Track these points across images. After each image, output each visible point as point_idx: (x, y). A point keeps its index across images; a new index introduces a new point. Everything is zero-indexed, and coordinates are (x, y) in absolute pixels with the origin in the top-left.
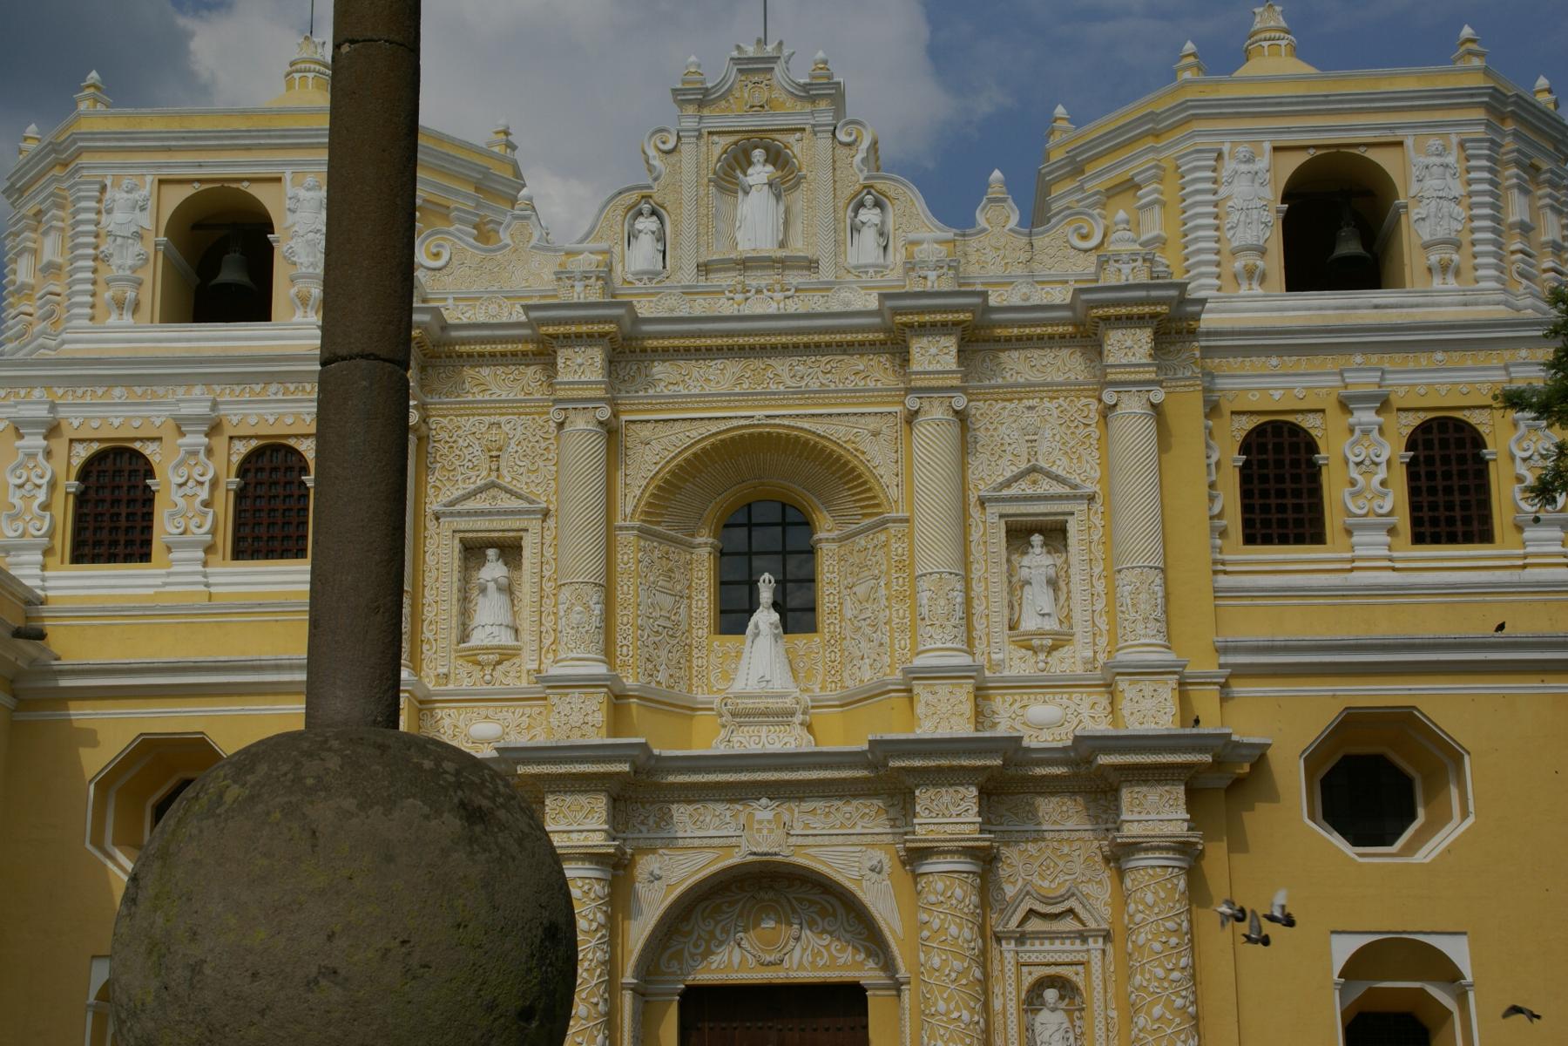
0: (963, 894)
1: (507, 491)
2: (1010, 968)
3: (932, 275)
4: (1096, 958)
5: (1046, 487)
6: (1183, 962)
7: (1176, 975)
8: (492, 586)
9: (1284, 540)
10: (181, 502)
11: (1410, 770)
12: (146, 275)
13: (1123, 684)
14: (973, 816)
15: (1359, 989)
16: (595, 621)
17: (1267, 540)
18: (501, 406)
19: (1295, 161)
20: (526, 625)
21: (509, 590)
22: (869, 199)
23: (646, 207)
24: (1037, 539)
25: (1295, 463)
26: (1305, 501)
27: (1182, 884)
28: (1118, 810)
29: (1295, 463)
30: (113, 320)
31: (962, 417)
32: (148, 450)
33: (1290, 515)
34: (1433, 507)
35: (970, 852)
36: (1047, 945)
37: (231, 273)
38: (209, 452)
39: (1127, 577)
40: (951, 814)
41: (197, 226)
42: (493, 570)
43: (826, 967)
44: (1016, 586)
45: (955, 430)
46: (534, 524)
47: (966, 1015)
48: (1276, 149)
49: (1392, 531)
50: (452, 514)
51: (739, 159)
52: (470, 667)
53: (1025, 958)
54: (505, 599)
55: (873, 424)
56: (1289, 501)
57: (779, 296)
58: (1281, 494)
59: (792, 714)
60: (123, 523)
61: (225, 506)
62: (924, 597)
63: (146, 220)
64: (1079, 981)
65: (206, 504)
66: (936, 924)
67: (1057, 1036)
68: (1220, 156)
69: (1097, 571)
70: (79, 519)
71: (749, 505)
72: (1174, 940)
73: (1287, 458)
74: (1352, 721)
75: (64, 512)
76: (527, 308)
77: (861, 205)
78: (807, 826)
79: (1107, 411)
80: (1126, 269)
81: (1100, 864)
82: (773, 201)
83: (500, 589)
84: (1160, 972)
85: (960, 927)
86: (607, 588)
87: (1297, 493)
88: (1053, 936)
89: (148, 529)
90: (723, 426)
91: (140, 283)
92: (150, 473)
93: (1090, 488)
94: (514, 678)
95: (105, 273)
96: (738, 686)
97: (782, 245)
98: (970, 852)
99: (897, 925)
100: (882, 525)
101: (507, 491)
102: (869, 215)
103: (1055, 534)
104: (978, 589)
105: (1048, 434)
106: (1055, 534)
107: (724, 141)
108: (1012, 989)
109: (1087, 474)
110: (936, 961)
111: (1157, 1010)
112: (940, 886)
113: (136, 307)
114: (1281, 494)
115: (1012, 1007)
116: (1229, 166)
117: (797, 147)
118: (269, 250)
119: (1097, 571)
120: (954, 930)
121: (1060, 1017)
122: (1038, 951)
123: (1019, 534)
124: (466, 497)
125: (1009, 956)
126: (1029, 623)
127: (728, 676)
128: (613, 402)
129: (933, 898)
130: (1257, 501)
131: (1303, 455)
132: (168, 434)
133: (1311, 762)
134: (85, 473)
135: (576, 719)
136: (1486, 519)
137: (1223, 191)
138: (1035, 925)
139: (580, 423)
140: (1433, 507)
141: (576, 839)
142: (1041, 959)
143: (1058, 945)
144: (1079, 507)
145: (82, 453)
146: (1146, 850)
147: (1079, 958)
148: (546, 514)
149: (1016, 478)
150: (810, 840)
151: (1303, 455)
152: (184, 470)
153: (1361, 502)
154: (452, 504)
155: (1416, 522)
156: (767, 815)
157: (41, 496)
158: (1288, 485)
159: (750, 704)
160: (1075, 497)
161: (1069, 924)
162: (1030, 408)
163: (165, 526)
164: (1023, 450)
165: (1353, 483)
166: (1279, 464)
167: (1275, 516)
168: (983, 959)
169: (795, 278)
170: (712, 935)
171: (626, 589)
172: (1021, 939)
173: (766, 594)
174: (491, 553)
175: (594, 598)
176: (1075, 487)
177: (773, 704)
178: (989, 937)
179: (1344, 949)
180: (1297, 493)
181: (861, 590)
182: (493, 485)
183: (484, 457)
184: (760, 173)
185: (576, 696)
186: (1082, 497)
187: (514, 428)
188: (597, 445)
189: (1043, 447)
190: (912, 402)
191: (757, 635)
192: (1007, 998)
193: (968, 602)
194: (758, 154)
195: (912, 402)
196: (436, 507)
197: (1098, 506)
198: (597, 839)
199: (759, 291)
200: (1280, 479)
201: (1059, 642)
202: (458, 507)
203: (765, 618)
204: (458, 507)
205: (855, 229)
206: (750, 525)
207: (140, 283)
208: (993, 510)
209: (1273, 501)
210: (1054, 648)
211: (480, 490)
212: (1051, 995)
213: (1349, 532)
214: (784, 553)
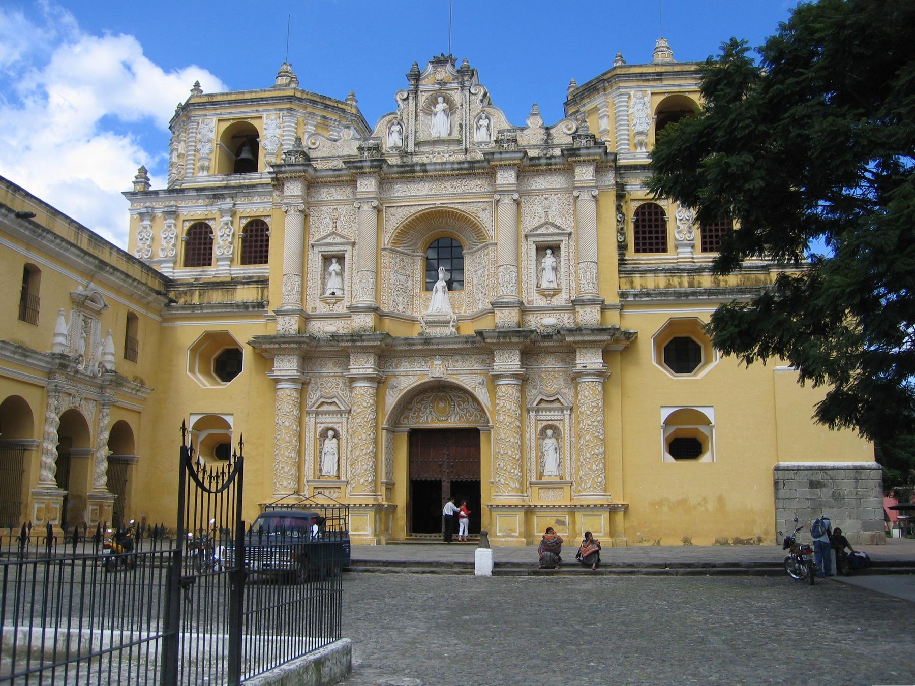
0: (514, 392)
1: (339, 235)
2: (533, 422)
3: (506, 145)
4: (567, 417)
5: (552, 230)
6: (599, 419)
7: (596, 423)
8: (334, 273)
9: (651, 251)
10: (221, 243)
12: (212, 156)
13: (578, 308)
15: (672, 429)
16: (371, 286)
17: (644, 251)
18: (338, 202)
19: (660, 99)
20: (346, 288)
21: (341, 274)
22: (484, 116)
23: (395, 122)
24: (549, 251)
25: (656, 220)
26: (660, 235)
27: (600, 389)
29: (656, 220)
30: (200, 174)
31: (518, 203)
32: (211, 223)
33: (654, 241)
34: (711, 237)
35: (515, 376)
36: (548, 413)
37: (245, 155)
38: (232, 222)
40: (508, 362)
41: (234, 137)
42: (335, 267)
43: (464, 422)
44: (540, 270)
45: (515, 206)
46: (349, 248)
47: (512, 440)
48: (652, 94)
49: (693, 247)
50: (318, 245)
52: (324, 305)
53: (539, 418)
54: (339, 279)
55: (483, 206)
56: (654, 235)
57: (447, 155)
58: (650, 232)
59: (449, 322)
60: (202, 251)
61: (238, 244)
62: (500, 275)
63: (212, 136)
64: (560, 426)
65: (231, 243)
66: (502, 404)
67: (552, 448)
68: (629, 97)
70: (187, 250)
71: (438, 240)
72: (595, 410)
73: (653, 217)
74: (673, 324)
75: (181, 249)
76: (344, 162)
78: (454, 366)
80: (583, 141)
81: (570, 382)
82: (445, 118)
83: (337, 274)
84: (589, 423)
85: (511, 406)
86: (377, 273)
87: (657, 232)
88: (550, 410)
89: (211, 254)
90: (424, 208)
91: (210, 160)
93: (569, 230)
94: (341, 308)
95: (198, 156)
96: (429, 311)
97: (450, 135)
98: (515, 376)
99: (489, 406)
100: (486, 246)
101: (339, 235)
102: (484, 122)
103: (555, 249)
104: (524, 271)
105: (553, 209)
106: (555, 249)
107: (426, 95)
108: (533, 430)
109: (567, 225)
110: (501, 419)
111: (587, 438)
112: (503, 389)
113: (208, 168)
114: (650, 232)
115: (533, 437)
116: (633, 100)
117: (457, 97)
118: (257, 144)
120: (508, 407)
121: (553, 440)
122: (544, 415)
123: (541, 249)
124: (324, 238)
125: (533, 417)
126: (545, 285)
127: (427, 307)
129: (500, 394)
130: (641, 236)
131: (660, 217)
132: (217, 216)
133: (657, 339)
134: (189, 233)
135: (362, 324)
137: (630, 112)
138: (543, 405)
139: (366, 207)
140: (711, 237)
141: (362, 371)
142: (546, 418)
143: (552, 413)
145: (188, 225)
146: (586, 375)
147: (560, 418)
148: (354, 244)
149: (541, 226)
150: (455, 372)
151: (660, 217)
152: (223, 230)
153: (681, 235)
154: (318, 241)
155: (704, 243)
156: (440, 362)
157: (173, 241)
158: (653, 229)
159: (431, 319)
160: (563, 234)
161: (556, 405)
162: (546, 199)
163: (216, 252)
164: (543, 216)
165: (678, 228)
166: (650, 220)
167: (648, 241)
168: (521, 419)
169: (453, 148)
170: (420, 409)
171: (384, 273)
172: (537, 411)
174: (334, 260)
175: (370, 277)
176: (564, 230)
177: (442, 318)
178: (525, 409)
179: (665, 413)
180: (657, 232)
181: (479, 273)
182: (334, 233)
183: (331, 222)
184: (441, 106)
185: (362, 316)
186: (565, 234)
187: (343, 210)
188: (373, 216)
189: (550, 214)
190: (497, 197)
191: (436, 291)
192: (531, 434)
193: (519, 277)
194: (440, 99)
195: (497, 197)
198: (370, 371)
199: (439, 154)
200: (650, 226)
201: (556, 292)
203: (441, 284)
205: (478, 128)
206: (438, 247)
207: (210, 160)
208: (531, 239)
209: (647, 235)
210: (554, 295)
211: (329, 235)
212: (549, 432)
213: (676, 247)
214: (452, 258)
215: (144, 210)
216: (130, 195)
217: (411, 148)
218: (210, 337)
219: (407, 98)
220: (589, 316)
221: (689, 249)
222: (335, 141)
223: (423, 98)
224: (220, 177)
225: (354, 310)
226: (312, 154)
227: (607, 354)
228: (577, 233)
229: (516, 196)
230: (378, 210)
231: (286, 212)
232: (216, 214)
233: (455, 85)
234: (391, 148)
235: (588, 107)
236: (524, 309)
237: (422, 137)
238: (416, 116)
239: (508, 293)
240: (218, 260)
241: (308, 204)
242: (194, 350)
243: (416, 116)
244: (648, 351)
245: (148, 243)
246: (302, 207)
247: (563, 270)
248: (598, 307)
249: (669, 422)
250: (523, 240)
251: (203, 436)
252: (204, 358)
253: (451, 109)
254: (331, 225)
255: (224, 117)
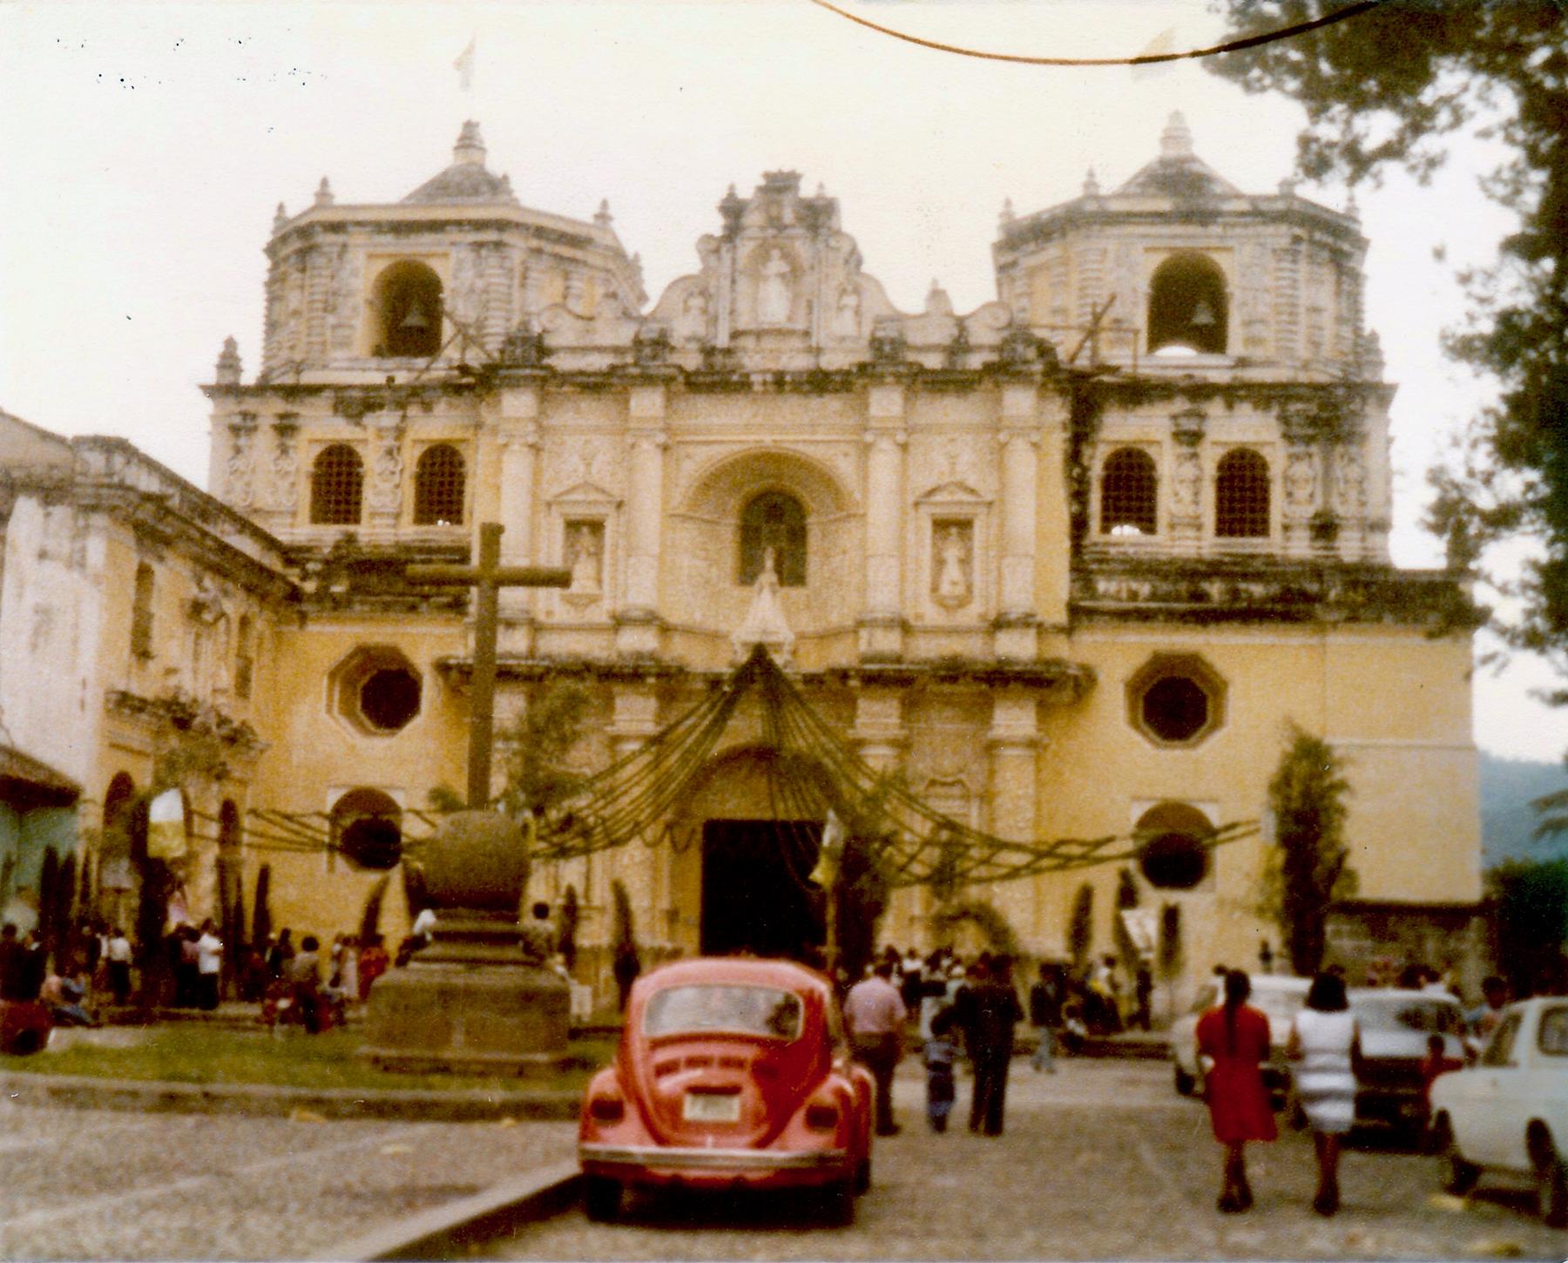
11: (1205, 691)
14: (895, 720)
22: (850, 288)
28: (991, 717)
31: (904, 447)
32: (359, 449)
35: (893, 743)
37: (414, 320)
38: (399, 449)
39: (1006, 561)
42: (586, 539)
44: (939, 563)
46: (610, 510)
49: (1199, 527)
50: (560, 503)
51: (762, 253)
55: (843, 447)
62: (871, 574)
65: (397, 486)
69: (992, 554)
75: (304, 494)
77: (844, 292)
79: (1003, 446)
83: (589, 554)
90: (746, 447)
92: (360, 464)
93: (989, 498)
97: (790, 319)
98: (893, 743)
100: (849, 516)
102: (851, 300)
103: (965, 525)
109: (986, 486)
119: (992, 554)
123: (942, 525)
124: (568, 492)
128: (667, 429)
134: (318, 463)
136: (1265, 522)
139: (645, 445)
144: (982, 510)
145: (317, 450)
148: (620, 505)
161: (956, 791)
162: (952, 440)
169: (797, 343)
173: (769, 563)
174: (585, 530)
179: (1137, 812)
184: (776, 265)
189: (959, 468)
191: (761, 590)
194: (775, 253)
196: (548, 498)
197: (995, 510)
201: (963, 602)
202: (565, 498)
204: (565, 498)
205: (840, 309)
213: (1172, 527)
215: (237, 420)
216: (213, 391)
217: (722, 341)
218: (366, 656)
219: (717, 251)
220: (1018, 647)
221: (1191, 533)
222: (591, 319)
223: (745, 248)
224: (374, 362)
225: (620, 622)
226: (550, 341)
227: (1045, 711)
228: (1002, 502)
229: (901, 437)
230: (665, 448)
231: (506, 445)
232: (370, 434)
233: (800, 231)
234: (689, 339)
235: (1032, 261)
236: (905, 627)
237: (743, 323)
238: (733, 282)
239: (883, 600)
240: (373, 515)
241: (541, 429)
242: (332, 676)
243: (733, 282)
244: (1112, 704)
245: (246, 478)
246: (531, 439)
247: (977, 564)
248: (1033, 632)
249: (1144, 823)
250: (912, 512)
251: (348, 821)
252: (349, 683)
253: (794, 274)
254: (582, 468)
255: (379, 250)
